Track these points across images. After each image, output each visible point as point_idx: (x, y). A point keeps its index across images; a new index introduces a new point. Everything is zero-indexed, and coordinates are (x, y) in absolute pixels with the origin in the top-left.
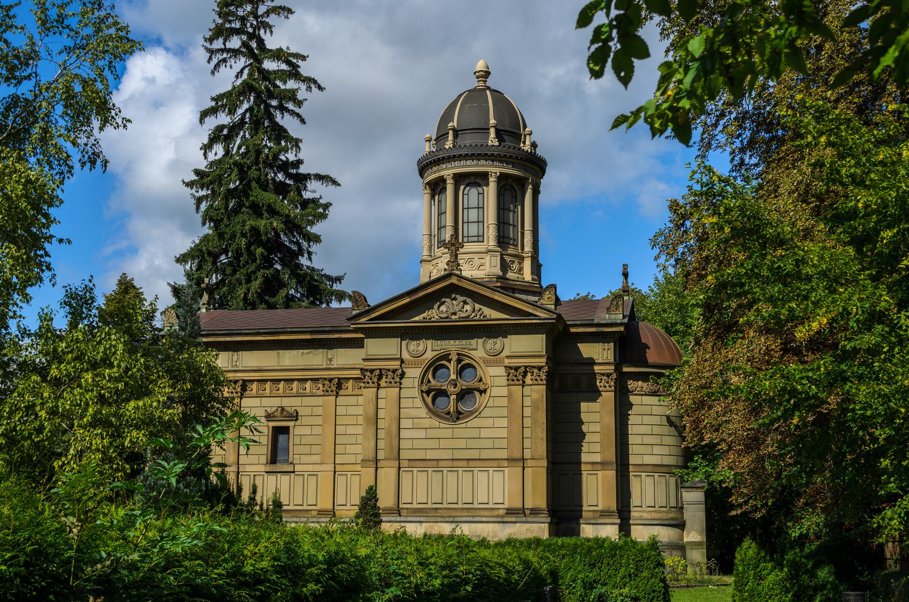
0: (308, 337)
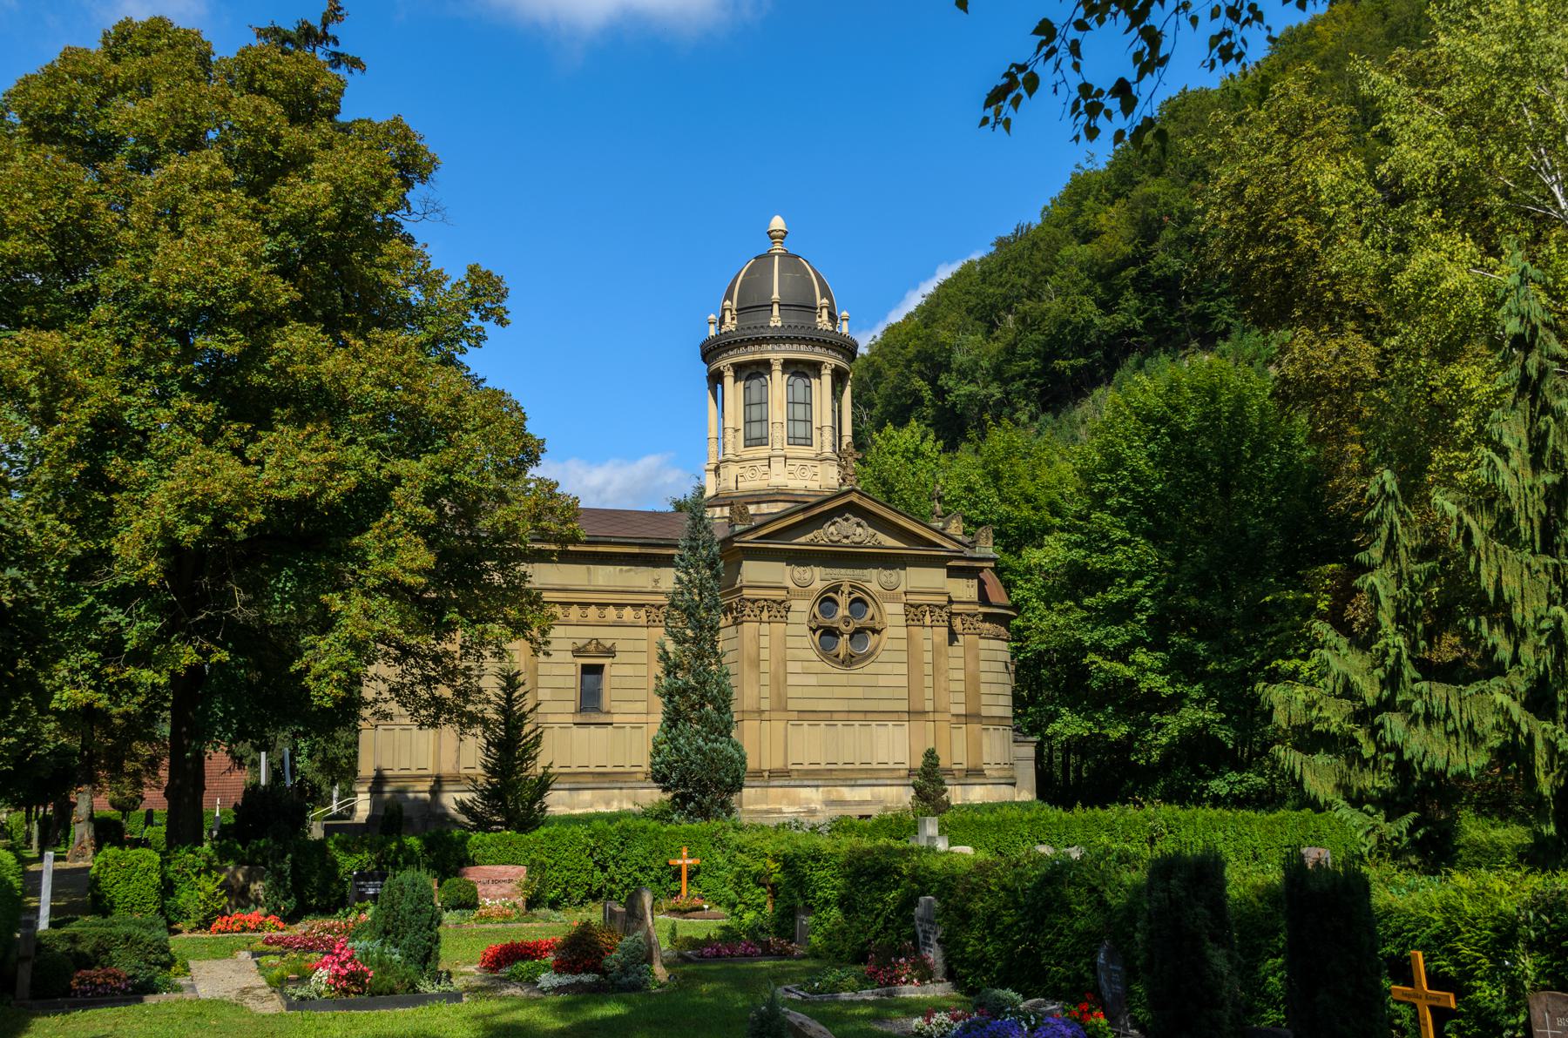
0: (636, 550)
